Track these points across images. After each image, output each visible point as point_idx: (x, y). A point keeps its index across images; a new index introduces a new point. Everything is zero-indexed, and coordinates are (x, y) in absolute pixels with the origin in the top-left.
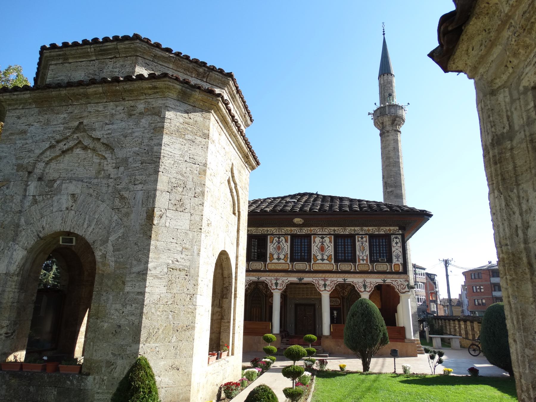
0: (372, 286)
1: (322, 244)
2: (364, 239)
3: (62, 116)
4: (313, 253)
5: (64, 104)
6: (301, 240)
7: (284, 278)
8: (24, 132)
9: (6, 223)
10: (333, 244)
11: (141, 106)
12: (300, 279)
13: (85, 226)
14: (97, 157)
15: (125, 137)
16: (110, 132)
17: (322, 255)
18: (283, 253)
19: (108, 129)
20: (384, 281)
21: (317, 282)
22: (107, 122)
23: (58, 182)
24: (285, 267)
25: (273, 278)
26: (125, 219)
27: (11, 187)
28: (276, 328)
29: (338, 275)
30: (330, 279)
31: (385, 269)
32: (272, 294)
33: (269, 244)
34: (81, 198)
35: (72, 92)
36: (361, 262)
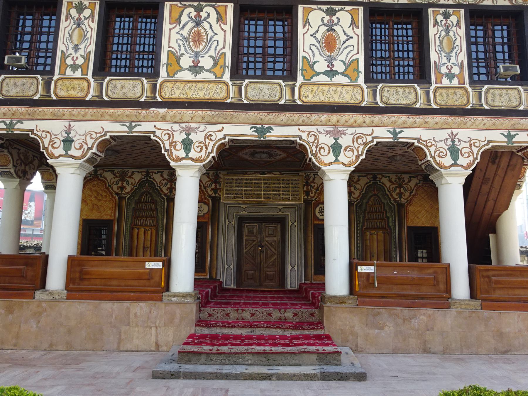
0: (475, 150)
1: (331, 29)
2: (453, 19)
4: (301, 54)
6: (265, 25)
7: (211, 128)
10: (360, 31)
12: (262, 131)
17: (330, 61)
18: (212, 53)
20: (510, 137)
21: (312, 139)
24: (217, 93)
25: (176, 126)
28: (183, 276)
29: (377, 118)
30: (351, 130)
31: (514, 103)
32: (172, 177)
33: (167, 25)
36: (446, 82)
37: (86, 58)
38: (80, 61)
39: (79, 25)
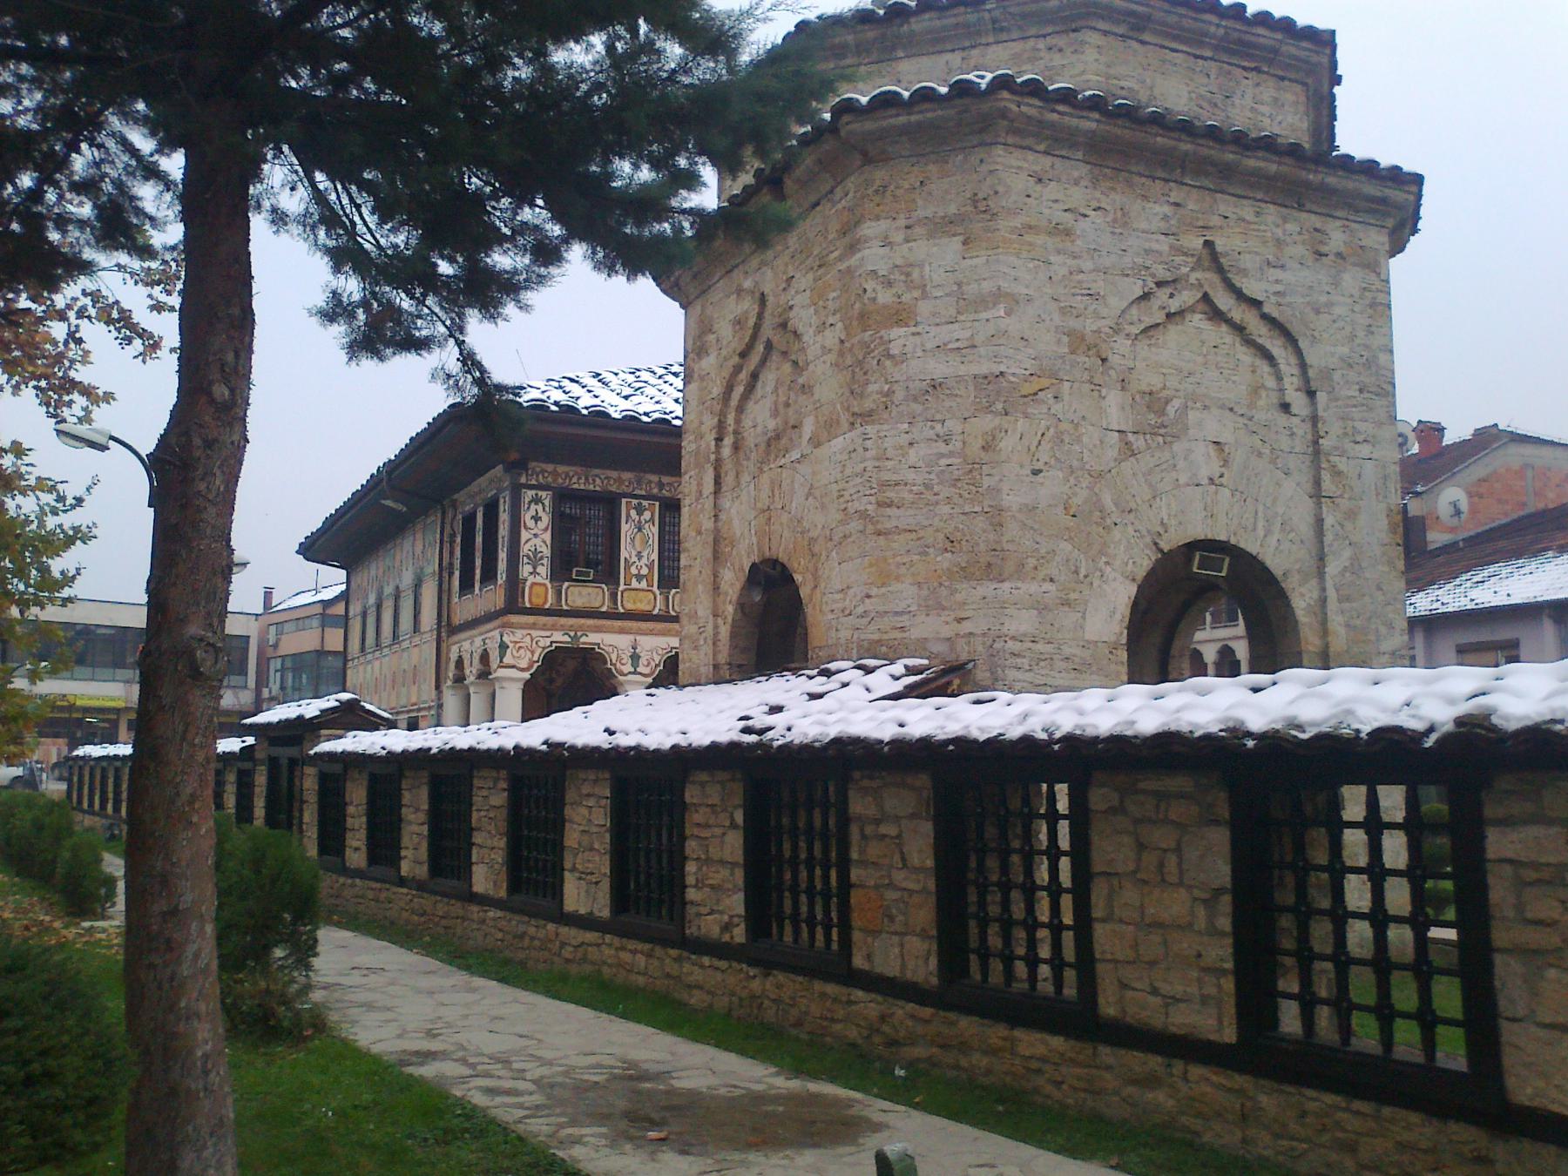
3: (1158, 208)
5: (1160, 174)
8: (1068, 233)
9: (1076, 501)
11: (1337, 238)
13: (1261, 533)
14: (1244, 349)
15: (1318, 312)
16: (1279, 288)
19: (1277, 281)
22: (1271, 258)
23: (1176, 403)
26: (1349, 526)
27: (1066, 397)
34: (1238, 457)
35: (1205, 152)
37: (650, 567)
38: (645, 571)
39: (640, 530)
